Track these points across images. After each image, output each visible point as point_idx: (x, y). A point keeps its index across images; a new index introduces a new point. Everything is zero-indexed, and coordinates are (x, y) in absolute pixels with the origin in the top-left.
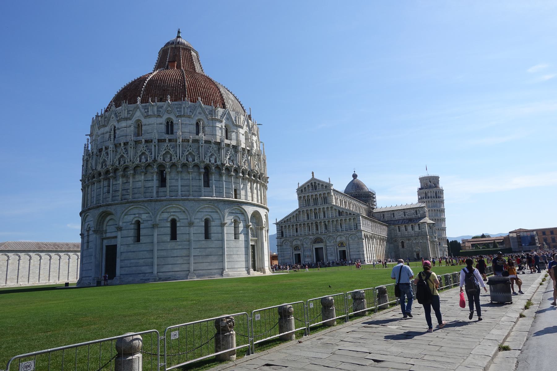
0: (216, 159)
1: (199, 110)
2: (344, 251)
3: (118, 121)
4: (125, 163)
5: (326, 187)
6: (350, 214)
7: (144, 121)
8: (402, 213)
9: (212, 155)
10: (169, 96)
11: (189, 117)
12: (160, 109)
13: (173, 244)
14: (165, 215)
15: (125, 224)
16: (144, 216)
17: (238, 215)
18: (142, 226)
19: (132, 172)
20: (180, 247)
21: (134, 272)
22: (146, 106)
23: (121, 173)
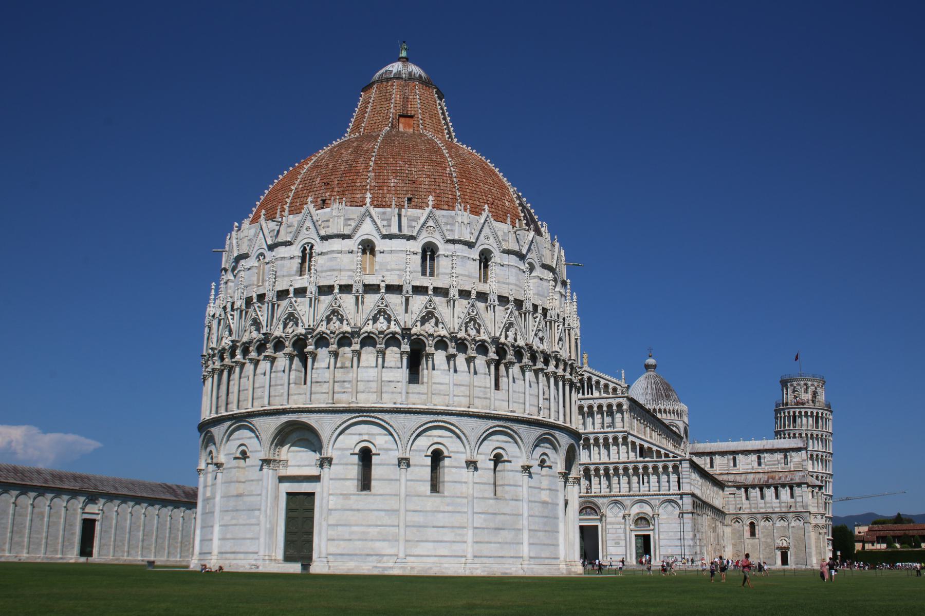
1: (486, 230)
2: (646, 539)
5: (615, 390)
6: (667, 456)
7: (380, 244)
8: (754, 457)
10: (431, 198)
11: (471, 245)
12: (414, 224)
13: (434, 502)
14: (424, 442)
15: (339, 452)
18: (375, 459)
20: (450, 508)
21: (358, 552)
22: (384, 213)
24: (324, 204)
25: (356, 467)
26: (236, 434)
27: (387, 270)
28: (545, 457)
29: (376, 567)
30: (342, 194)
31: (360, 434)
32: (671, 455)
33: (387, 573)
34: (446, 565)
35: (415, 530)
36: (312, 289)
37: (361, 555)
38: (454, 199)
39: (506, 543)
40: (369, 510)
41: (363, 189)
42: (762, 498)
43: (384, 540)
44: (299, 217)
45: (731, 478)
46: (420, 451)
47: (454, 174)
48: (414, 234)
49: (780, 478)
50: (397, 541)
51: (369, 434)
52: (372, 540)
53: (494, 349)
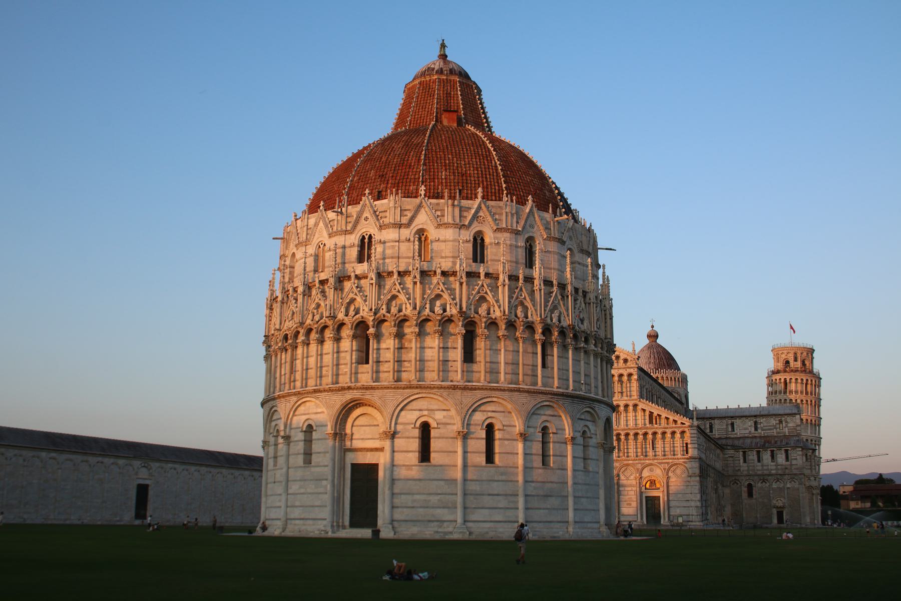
0: (559, 317)
3: (381, 228)
4: (400, 311)
8: (750, 423)
9: (555, 308)
12: (465, 214)
13: (491, 469)
14: (478, 417)
16: (439, 415)
17: (589, 424)
18: (433, 433)
19: (417, 330)
20: (504, 478)
21: (420, 518)
22: (438, 204)
23: (394, 330)
24: (379, 196)
25: (417, 440)
26: (302, 409)
27: (442, 257)
28: (586, 429)
29: (437, 532)
30: (397, 186)
31: (420, 410)
32: (679, 422)
33: (448, 537)
34: (501, 530)
35: (471, 498)
36: (373, 275)
37: (423, 521)
38: (501, 191)
39: (554, 509)
40: (430, 480)
41: (416, 182)
42: (759, 461)
43: (444, 508)
44: (358, 208)
45: (730, 442)
46: (476, 425)
47: (500, 168)
48: (467, 223)
49: (776, 442)
50: (456, 508)
51: (428, 410)
52: (433, 507)
53: (540, 331)
